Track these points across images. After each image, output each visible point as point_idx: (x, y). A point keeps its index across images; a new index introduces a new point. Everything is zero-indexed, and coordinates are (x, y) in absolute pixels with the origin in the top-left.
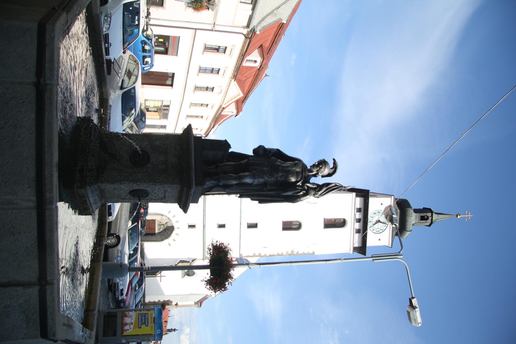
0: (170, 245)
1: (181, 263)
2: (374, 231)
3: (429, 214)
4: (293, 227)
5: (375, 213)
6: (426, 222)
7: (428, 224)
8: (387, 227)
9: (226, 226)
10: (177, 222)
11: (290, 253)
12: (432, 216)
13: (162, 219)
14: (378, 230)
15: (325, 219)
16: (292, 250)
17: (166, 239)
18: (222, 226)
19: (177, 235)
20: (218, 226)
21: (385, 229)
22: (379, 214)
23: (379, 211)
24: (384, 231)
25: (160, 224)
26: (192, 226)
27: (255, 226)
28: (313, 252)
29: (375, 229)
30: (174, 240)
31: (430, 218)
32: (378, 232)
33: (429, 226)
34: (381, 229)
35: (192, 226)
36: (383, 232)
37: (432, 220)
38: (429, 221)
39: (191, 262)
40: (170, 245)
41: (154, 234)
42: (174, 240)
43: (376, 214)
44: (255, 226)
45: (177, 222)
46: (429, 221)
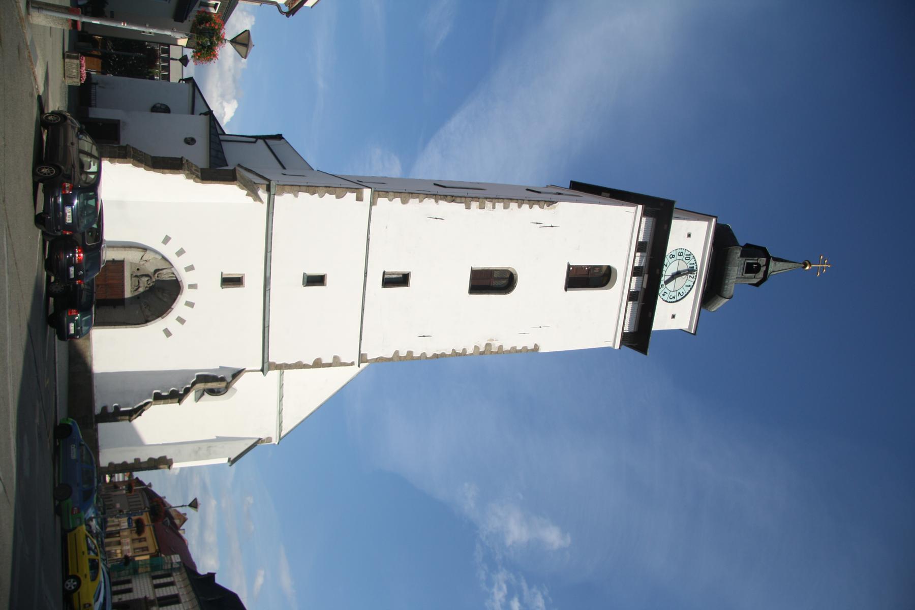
0: (168, 333)
1: (203, 384)
3: (762, 261)
4: (495, 283)
6: (755, 278)
7: (755, 281)
9: (328, 280)
10: (190, 268)
11: (482, 349)
12: (767, 265)
13: (144, 258)
14: (673, 294)
15: (569, 266)
16: (489, 342)
17: (158, 317)
19: (190, 304)
20: (306, 280)
21: (688, 293)
23: (681, 251)
24: (684, 297)
25: (139, 274)
27: (402, 280)
28: (536, 345)
29: (668, 292)
30: (181, 321)
31: (763, 269)
32: (673, 300)
33: (757, 285)
34: (679, 293)
36: (682, 298)
37: (766, 272)
38: (760, 275)
39: (229, 379)
40: (168, 333)
41: (120, 302)
42: (181, 321)
43: (675, 258)
44: (402, 280)
45: (190, 268)
46: (760, 275)
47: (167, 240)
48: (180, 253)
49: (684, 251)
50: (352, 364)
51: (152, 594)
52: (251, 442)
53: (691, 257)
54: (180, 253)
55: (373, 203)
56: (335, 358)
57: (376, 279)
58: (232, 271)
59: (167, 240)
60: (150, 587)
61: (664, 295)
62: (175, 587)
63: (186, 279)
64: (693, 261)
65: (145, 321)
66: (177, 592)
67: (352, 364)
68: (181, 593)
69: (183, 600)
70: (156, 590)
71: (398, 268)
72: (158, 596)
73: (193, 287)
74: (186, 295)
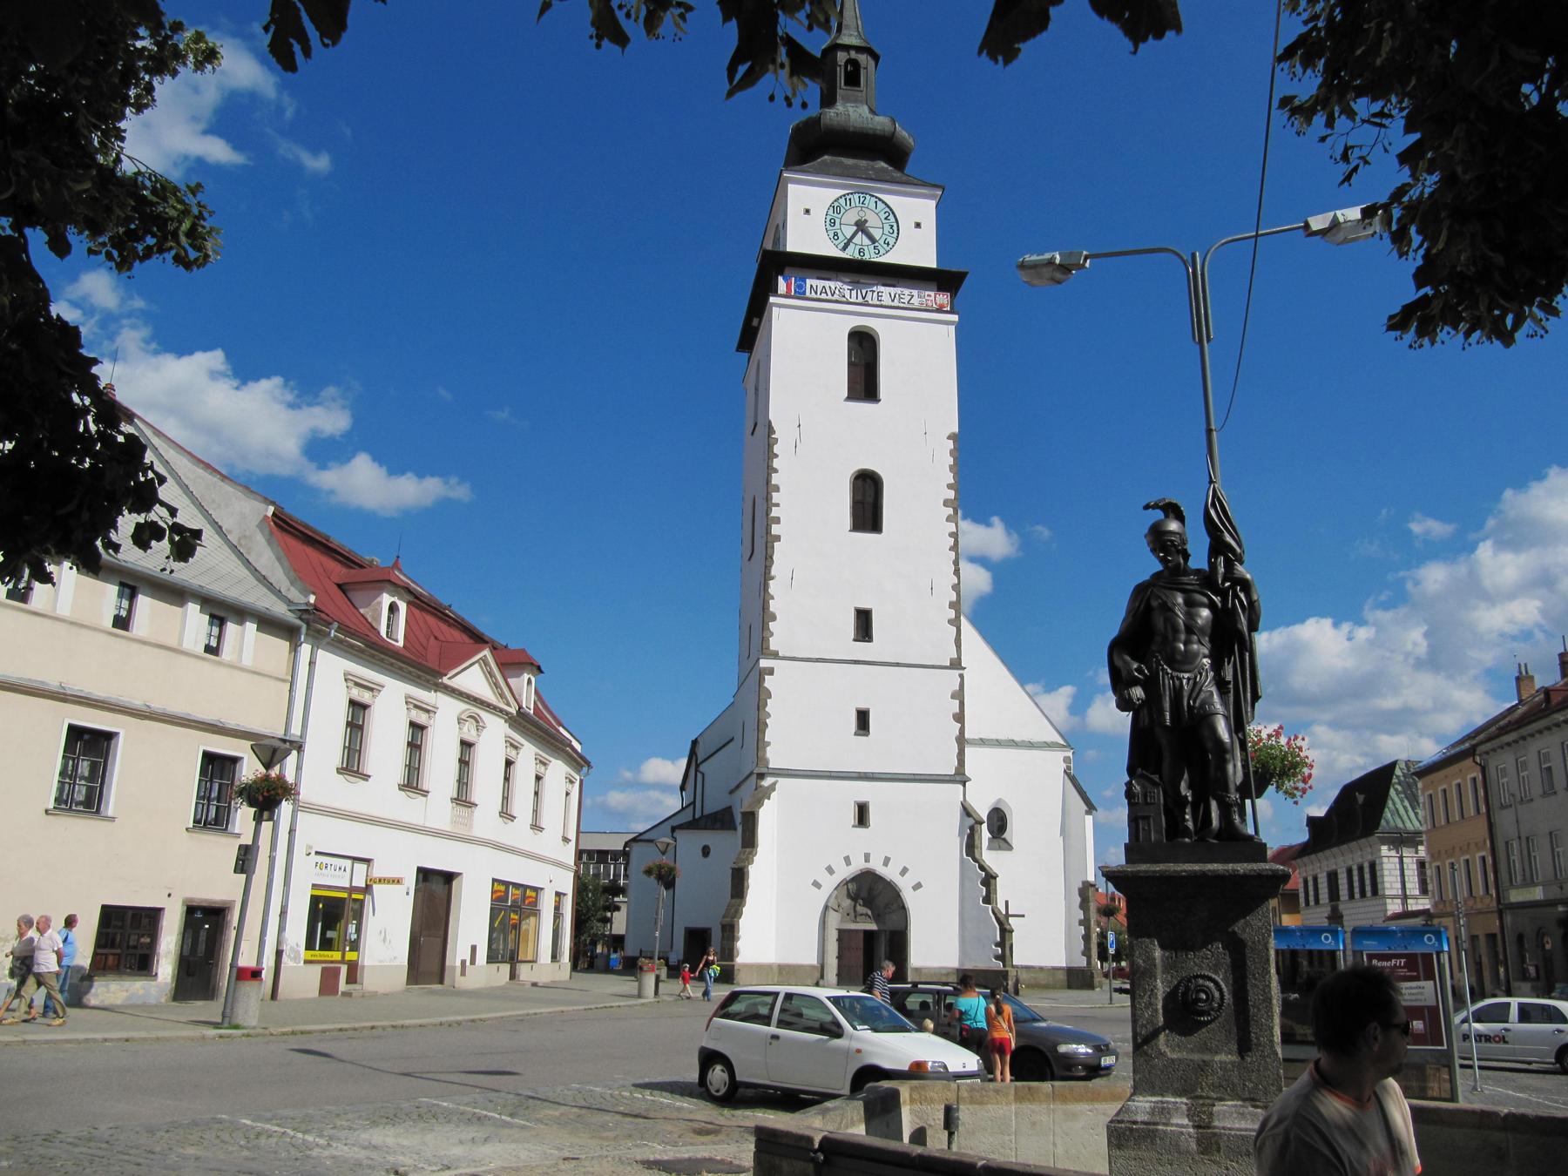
0: (918, 886)
2: (891, 243)
3: (842, 57)
4: (870, 499)
5: (836, 234)
6: (866, 68)
7: (872, 63)
8: (880, 200)
9: (863, 706)
10: (847, 860)
11: (950, 511)
12: (847, 48)
13: (836, 908)
14: (887, 228)
17: (899, 896)
18: (863, 720)
19: (887, 861)
20: (861, 732)
21: (886, 204)
22: (838, 221)
24: (891, 210)
25: (852, 914)
26: (862, 815)
28: (949, 438)
30: (904, 871)
31: (853, 54)
32: (895, 228)
33: (876, 57)
34: (886, 219)
35: (862, 815)
36: (893, 213)
37: (859, 49)
38: (863, 58)
40: (918, 886)
42: (904, 871)
43: (839, 231)
45: (847, 860)
46: (863, 58)
47: (817, 885)
48: (830, 870)
49: (829, 217)
50: (961, 676)
51: (1324, 909)
52: (1069, 785)
53: (836, 204)
54: (830, 870)
55: (775, 655)
56: (953, 696)
57: (863, 650)
58: (851, 815)
59: (817, 885)
60: (1318, 910)
61: (888, 244)
62: (1319, 876)
63: (858, 865)
64: (842, 201)
65: (903, 908)
66: (1325, 874)
67: (961, 676)
68: (1326, 869)
69: (1334, 867)
70: (1321, 902)
71: (849, 624)
72: (1327, 901)
73: (867, 858)
74: (877, 866)
